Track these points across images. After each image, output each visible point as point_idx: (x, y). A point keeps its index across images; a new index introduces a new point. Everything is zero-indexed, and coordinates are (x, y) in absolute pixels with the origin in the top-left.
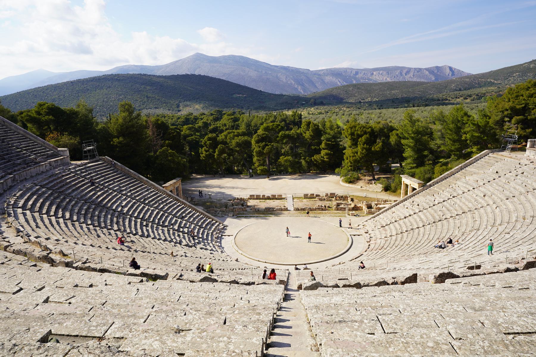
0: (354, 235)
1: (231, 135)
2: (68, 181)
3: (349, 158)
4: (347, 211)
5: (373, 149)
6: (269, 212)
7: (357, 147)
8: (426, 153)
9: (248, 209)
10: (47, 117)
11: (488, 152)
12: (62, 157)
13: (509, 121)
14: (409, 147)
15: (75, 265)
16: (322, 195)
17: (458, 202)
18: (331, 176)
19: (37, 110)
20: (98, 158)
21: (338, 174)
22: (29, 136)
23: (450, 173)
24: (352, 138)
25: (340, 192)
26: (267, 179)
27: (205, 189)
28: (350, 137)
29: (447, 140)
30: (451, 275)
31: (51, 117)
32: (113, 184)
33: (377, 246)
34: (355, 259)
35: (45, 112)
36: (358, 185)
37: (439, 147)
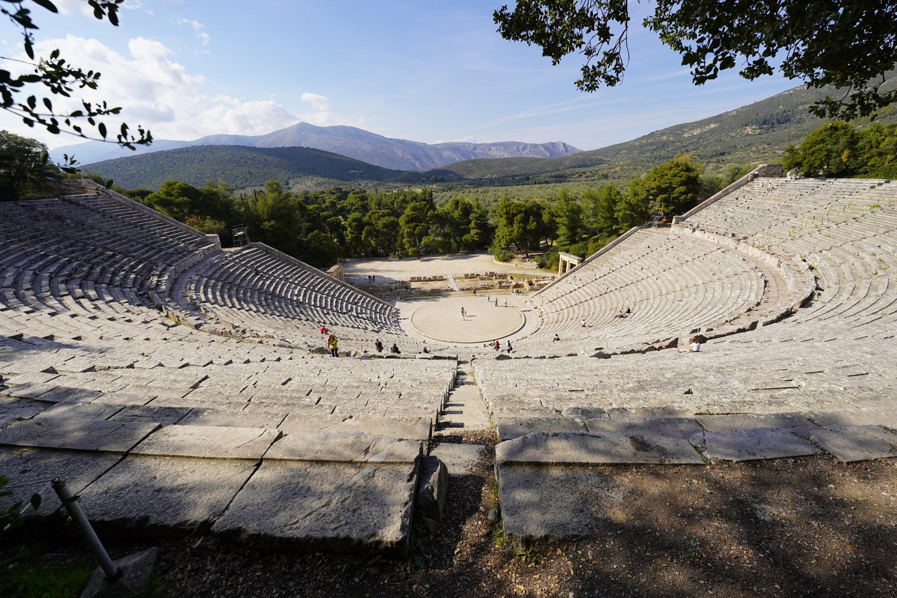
1: (376, 215)
2: (231, 270)
4: (511, 289)
5: (528, 228)
6: (435, 294)
7: (512, 226)
8: (579, 230)
9: (413, 291)
10: (181, 199)
12: (213, 245)
13: (654, 200)
14: (564, 225)
16: (483, 274)
17: (619, 275)
18: (482, 255)
19: (165, 190)
20: (250, 244)
21: (491, 253)
22: (167, 221)
26: (418, 261)
27: (360, 273)
29: (599, 217)
31: (185, 198)
32: (276, 272)
33: (551, 320)
35: (177, 192)
37: (592, 224)
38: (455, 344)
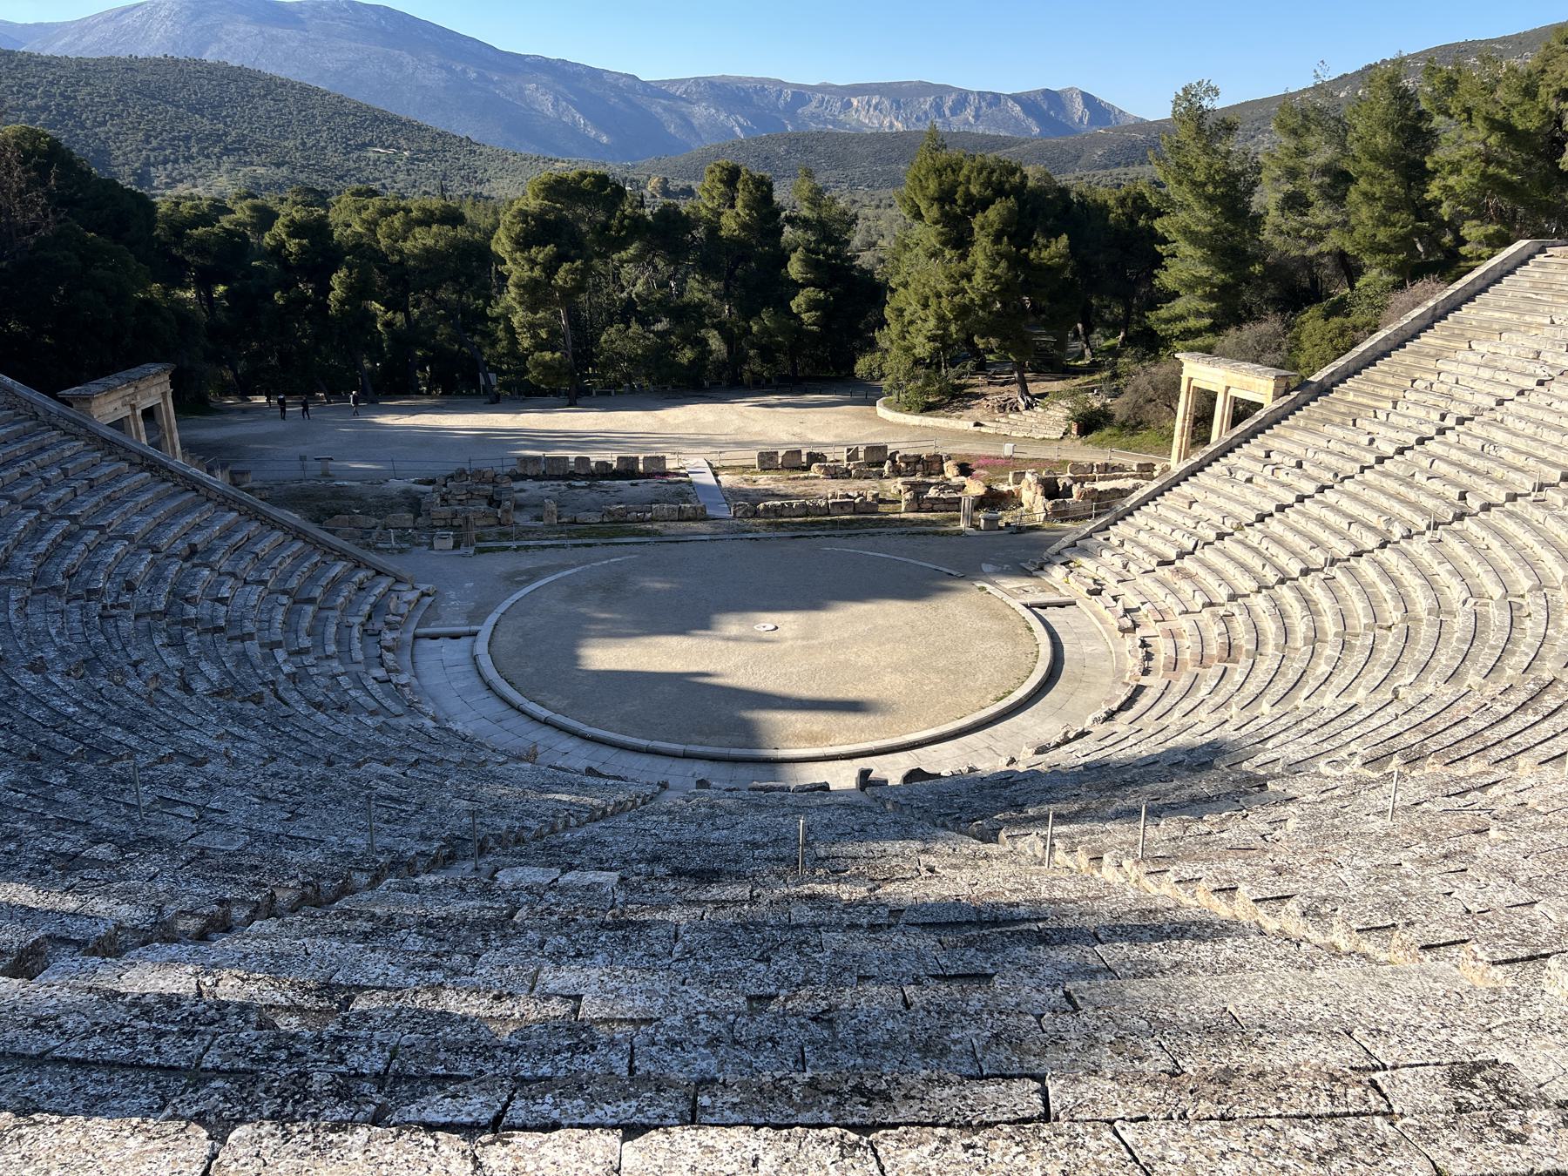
0: (1043, 607)
1: (397, 221)
3: (933, 301)
7: (963, 257)
11: (1531, 250)
14: (1193, 238)
16: (839, 455)
17: (1499, 436)
23: (1395, 333)
24: (944, 214)
25: (902, 446)
28: (935, 212)
34: (1121, 709)
36: (959, 417)
38: (702, 769)
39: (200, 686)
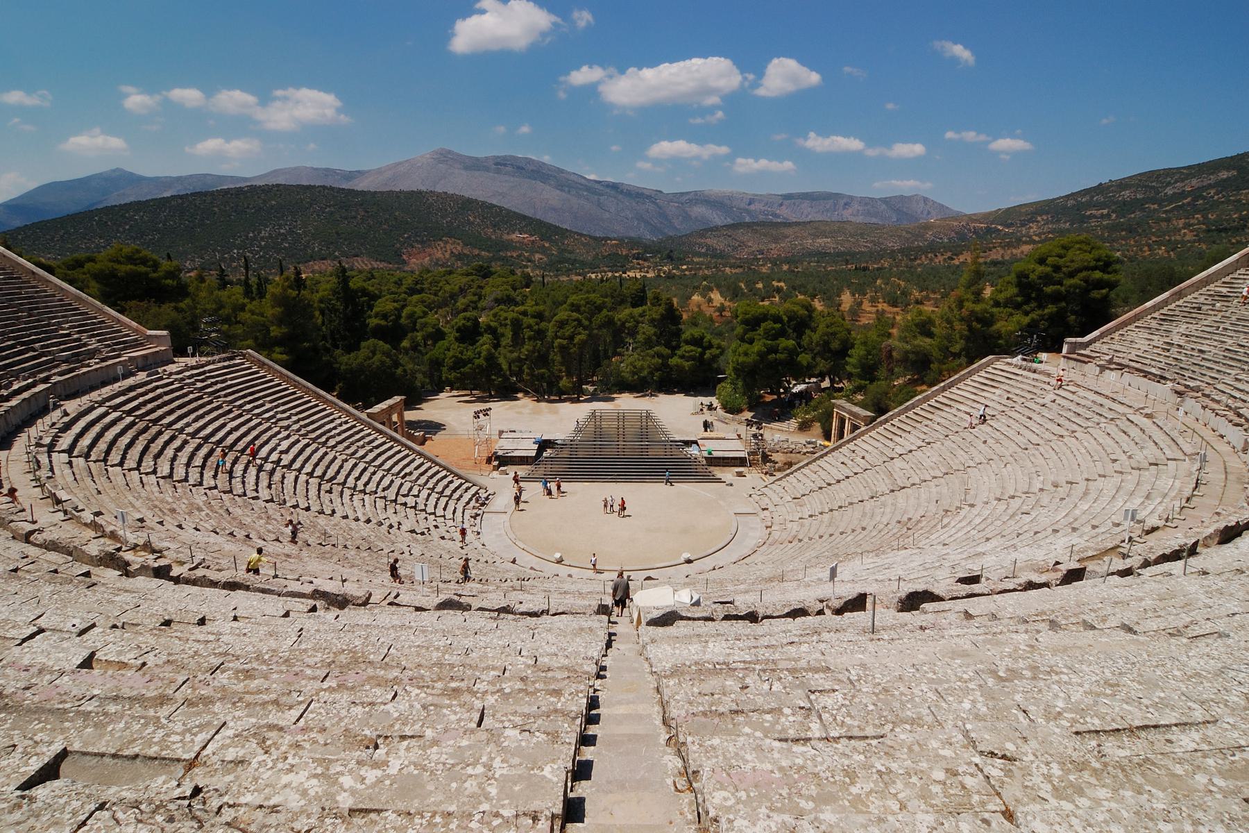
15: (174, 573)
30: (929, 597)
39: (403, 528)
